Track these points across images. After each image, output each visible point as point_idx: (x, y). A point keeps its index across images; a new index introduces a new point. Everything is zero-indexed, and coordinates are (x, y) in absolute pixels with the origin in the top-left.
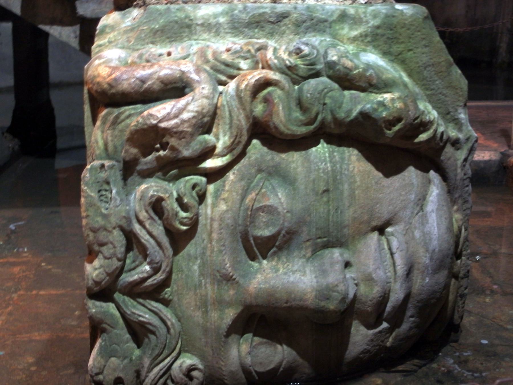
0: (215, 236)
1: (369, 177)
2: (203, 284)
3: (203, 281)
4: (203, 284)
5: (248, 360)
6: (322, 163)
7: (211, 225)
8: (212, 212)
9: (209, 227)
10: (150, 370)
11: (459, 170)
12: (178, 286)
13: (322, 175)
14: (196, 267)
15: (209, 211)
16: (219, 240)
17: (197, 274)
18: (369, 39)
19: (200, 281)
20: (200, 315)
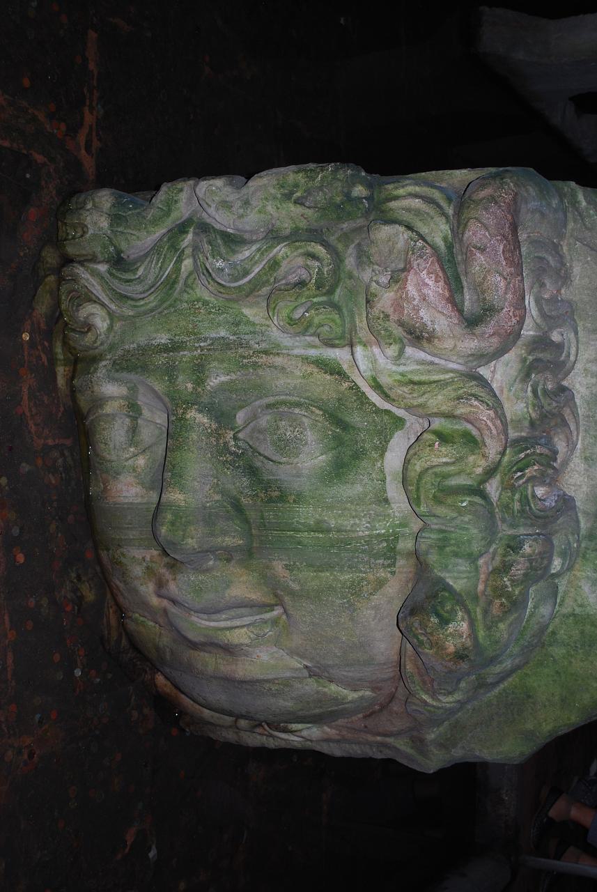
0: (264, 359)
1: (352, 595)
2: (202, 344)
3: (205, 344)
4: (202, 344)
5: (109, 409)
6: (369, 522)
7: (278, 354)
8: (297, 356)
9: (275, 351)
10: (94, 273)
11: (379, 738)
12: (199, 308)
13: (352, 522)
14: (223, 333)
15: (296, 352)
16: (255, 365)
17: (213, 335)
18: (578, 610)
19: (205, 340)
20: (163, 341)
